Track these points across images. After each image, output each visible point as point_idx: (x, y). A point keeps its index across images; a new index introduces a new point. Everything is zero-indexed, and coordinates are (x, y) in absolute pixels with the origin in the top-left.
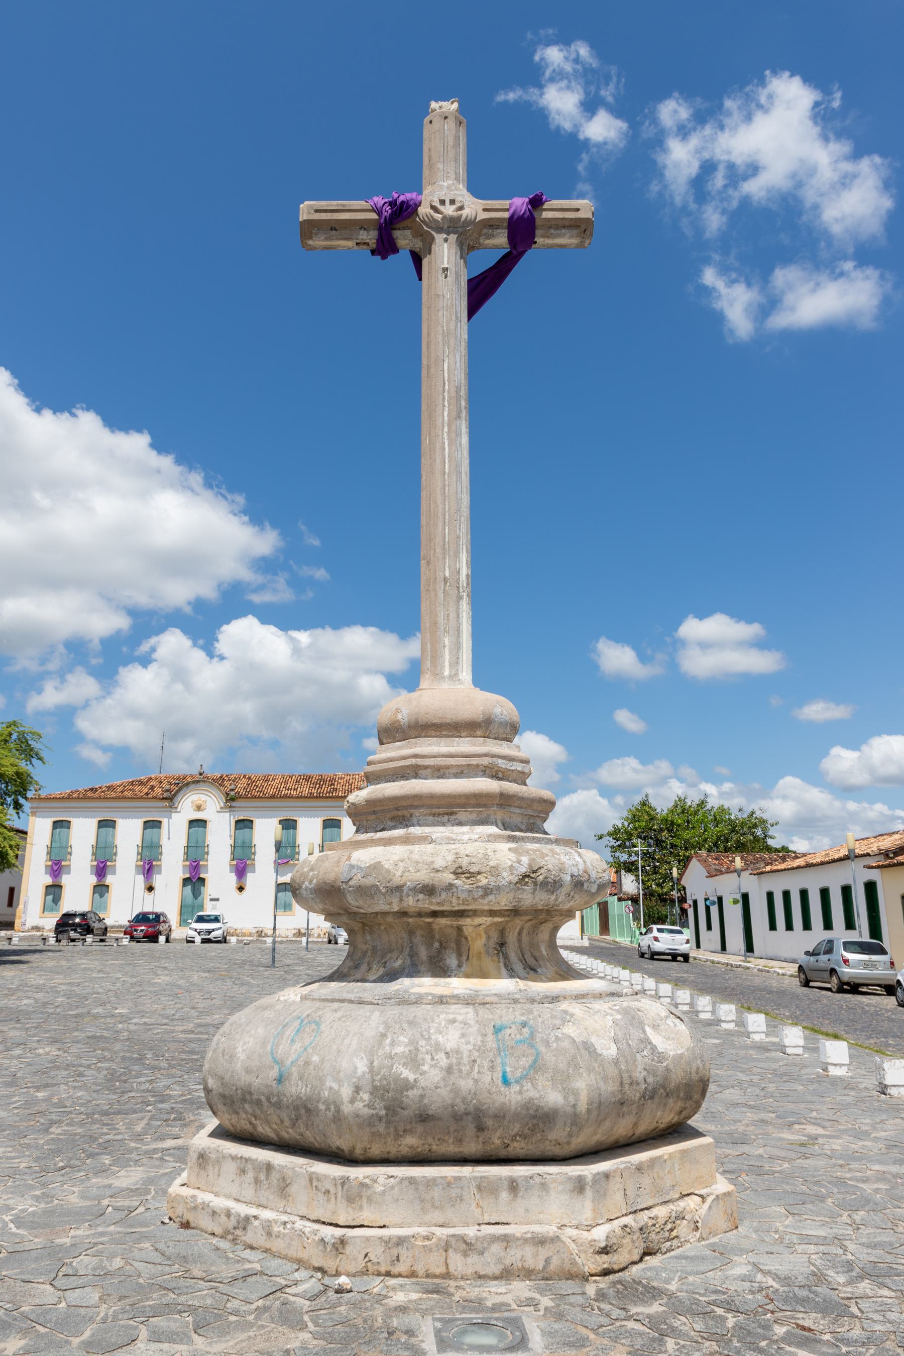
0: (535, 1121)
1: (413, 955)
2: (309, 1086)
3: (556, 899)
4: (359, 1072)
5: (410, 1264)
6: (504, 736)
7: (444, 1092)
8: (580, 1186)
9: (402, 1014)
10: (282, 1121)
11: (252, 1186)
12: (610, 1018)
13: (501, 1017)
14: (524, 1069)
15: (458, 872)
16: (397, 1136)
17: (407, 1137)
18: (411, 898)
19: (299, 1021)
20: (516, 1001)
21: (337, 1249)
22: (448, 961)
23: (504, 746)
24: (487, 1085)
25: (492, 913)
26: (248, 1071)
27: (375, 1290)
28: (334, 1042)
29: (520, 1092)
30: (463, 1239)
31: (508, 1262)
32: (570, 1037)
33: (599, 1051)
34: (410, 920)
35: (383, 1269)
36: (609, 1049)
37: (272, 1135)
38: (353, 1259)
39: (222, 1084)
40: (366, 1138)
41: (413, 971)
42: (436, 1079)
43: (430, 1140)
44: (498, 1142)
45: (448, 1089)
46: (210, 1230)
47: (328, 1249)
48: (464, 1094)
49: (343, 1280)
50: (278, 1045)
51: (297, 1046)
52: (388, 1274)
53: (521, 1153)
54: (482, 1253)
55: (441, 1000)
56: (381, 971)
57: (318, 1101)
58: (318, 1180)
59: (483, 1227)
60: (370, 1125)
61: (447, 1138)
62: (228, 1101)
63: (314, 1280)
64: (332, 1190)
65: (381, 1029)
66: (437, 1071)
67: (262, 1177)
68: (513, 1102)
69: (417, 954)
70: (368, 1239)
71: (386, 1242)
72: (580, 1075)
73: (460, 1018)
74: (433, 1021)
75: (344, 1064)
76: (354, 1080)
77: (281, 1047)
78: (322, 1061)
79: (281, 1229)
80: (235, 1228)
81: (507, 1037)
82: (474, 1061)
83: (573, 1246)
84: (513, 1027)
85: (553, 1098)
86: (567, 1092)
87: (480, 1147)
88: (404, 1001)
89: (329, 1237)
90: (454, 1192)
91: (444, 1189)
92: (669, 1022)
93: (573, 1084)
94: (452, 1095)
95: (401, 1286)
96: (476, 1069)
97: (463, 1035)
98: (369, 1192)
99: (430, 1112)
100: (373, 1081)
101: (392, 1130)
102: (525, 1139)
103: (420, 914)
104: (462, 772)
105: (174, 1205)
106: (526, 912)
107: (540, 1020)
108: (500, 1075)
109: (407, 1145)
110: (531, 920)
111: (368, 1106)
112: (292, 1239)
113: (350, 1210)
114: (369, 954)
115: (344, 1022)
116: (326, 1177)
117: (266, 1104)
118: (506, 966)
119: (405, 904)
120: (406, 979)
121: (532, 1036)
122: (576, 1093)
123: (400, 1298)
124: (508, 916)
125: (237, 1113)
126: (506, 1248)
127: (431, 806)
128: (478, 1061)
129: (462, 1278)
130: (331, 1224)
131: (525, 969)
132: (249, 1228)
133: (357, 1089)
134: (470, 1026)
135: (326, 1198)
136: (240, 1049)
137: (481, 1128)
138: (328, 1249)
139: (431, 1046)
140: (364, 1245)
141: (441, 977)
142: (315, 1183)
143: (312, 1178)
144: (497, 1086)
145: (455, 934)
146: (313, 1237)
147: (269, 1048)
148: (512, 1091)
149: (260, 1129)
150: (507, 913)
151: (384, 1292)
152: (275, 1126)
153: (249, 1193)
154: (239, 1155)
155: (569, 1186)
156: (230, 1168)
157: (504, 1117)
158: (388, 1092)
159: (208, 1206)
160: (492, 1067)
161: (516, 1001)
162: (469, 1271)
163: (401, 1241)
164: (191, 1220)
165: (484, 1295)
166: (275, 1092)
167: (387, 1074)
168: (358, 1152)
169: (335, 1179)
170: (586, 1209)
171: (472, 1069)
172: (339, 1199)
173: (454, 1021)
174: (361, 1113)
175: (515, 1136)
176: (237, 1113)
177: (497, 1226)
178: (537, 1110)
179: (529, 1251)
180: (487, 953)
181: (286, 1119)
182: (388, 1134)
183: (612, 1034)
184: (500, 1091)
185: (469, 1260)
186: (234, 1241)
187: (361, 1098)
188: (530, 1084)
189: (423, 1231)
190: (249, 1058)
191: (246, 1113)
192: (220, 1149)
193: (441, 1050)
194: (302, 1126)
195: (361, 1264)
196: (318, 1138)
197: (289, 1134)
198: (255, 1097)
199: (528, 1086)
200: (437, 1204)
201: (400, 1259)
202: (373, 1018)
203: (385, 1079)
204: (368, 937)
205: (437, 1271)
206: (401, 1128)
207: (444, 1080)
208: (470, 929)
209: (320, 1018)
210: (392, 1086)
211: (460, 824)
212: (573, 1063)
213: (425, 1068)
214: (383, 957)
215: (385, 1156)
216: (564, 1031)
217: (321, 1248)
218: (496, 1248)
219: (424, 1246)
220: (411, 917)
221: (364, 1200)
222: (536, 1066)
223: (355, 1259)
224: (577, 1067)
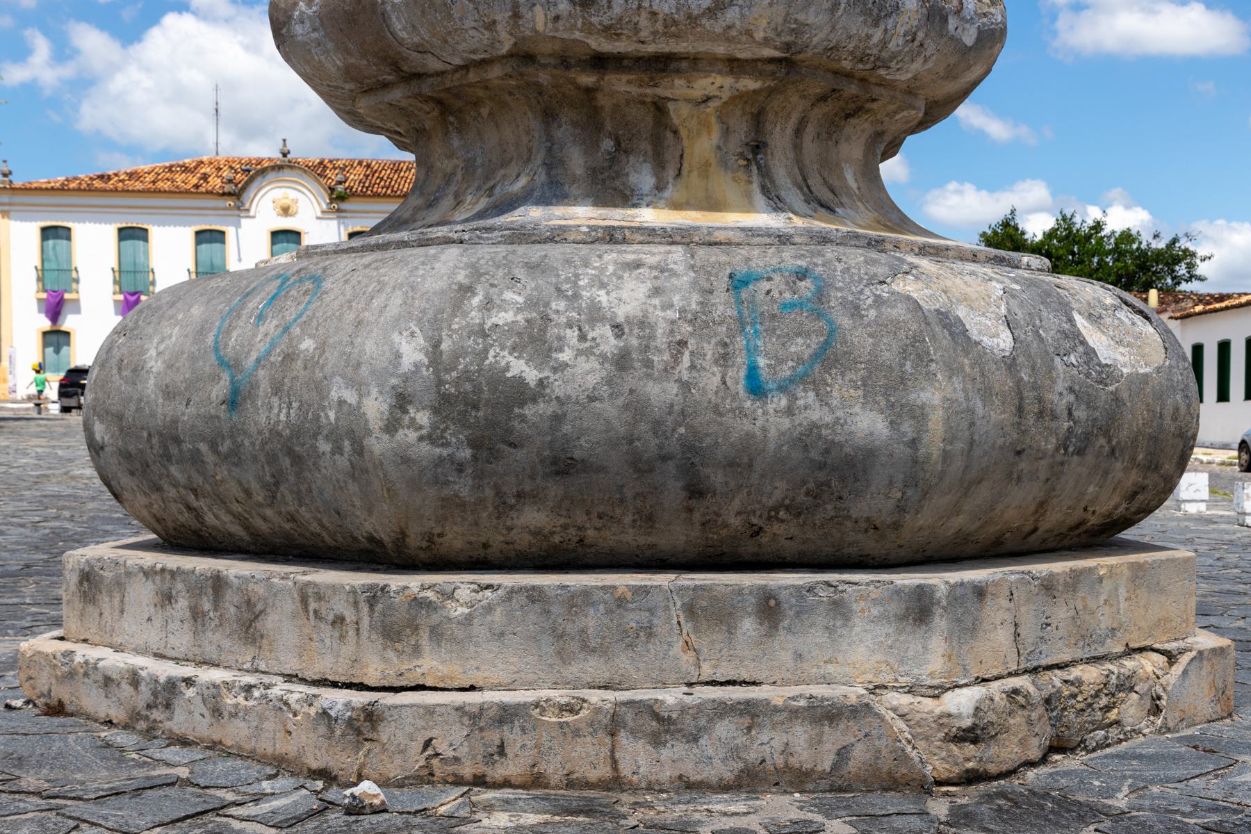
0: (821, 476)
2: (295, 405)
3: (884, 43)
4: (407, 363)
5: (531, 762)
7: (609, 409)
8: (919, 609)
9: (514, 252)
10: (248, 492)
11: (186, 626)
12: (1000, 286)
13: (749, 259)
14: (800, 361)
16: (503, 508)
17: (526, 508)
19: (279, 281)
21: (359, 732)
22: (633, 179)
24: (711, 395)
25: (734, 65)
26: (169, 393)
27: (442, 810)
28: (350, 308)
29: (790, 411)
30: (651, 710)
31: (753, 756)
32: (909, 298)
33: (975, 336)
35: (467, 771)
36: (997, 335)
37: (236, 529)
38: (399, 749)
39: (121, 430)
41: (554, 193)
42: (591, 381)
43: (580, 518)
44: (735, 522)
45: (620, 401)
46: (102, 715)
47: (338, 732)
49: (367, 787)
50: (228, 332)
51: (271, 326)
52: (480, 781)
53: (790, 549)
54: (694, 739)
55: (611, 236)
56: (483, 203)
57: (315, 436)
58: (320, 598)
59: (698, 688)
60: (436, 481)
61: (618, 512)
62: (138, 466)
63: (304, 792)
64: (350, 616)
65: (462, 277)
66: (593, 363)
67: (207, 605)
68: (773, 433)
69: (562, 162)
70: (430, 710)
71: (474, 718)
72: (930, 377)
74: (586, 265)
75: (370, 347)
76: (394, 381)
77: (235, 334)
78: (322, 347)
79: (241, 699)
80: (149, 707)
81: (761, 296)
82: (682, 343)
83: (900, 724)
84: (777, 278)
85: (868, 424)
86: (898, 412)
87: (695, 533)
88: (522, 236)
89: (340, 706)
90: (632, 619)
91: (609, 612)
93: (912, 396)
94: (627, 416)
95: (507, 802)
96: (686, 360)
97: (656, 291)
98: (435, 618)
99: (577, 454)
100: (440, 383)
101: (489, 493)
102: (799, 515)
103: (564, 61)
105: (32, 672)
107: (840, 267)
108: (743, 373)
109: (526, 528)
111: (430, 438)
112: (262, 718)
113: (391, 654)
114: (459, 176)
115: (377, 269)
116: (334, 588)
117: (210, 458)
118: (765, 191)
120: (534, 208)
121: (820, 295)
122: (919, 414)
125: (159, 489)
126: (749, 729)
128: (692, 343)
129: (649, 788)
130: (349, 686)
131: (807, 202)
132: (178, 704)
133: (402, 401)
134: (674, 274)
135: (337, 634)
136: (153, 352)
137: (696, 491)
138: (338, 732)
140: (421, 723)
141: (615, 206)
142: (313, 605)
143: (305, 595)
145: (649, 120)
146: (306, 709)
147: (210, 340)
148: (771, 408)
149: (210, 519)
150: (770, 67)
151: (463, 813)
152: (237, 508)
153: (182, 640)
154: (159, 566)
155: (895, 608)
156: (142, 593)
157: (750, 465)
158: (476, 407)
159: (95, 668)
160: (725, 357)
162: (666, 774)
163: (506, 715)
164: (66, 699)
165: (697, 816)
166: (225, 428)
167: (474, 368)
168: (414, 541)
169: (353, 591)
170: (932, 654)
171: (676, 358)
172: (365, 633)
173: (637, 265)
174: (412, 453)
175: (776, 509)
176: (159, 489)
177: (730, 688)
178: (827, 451)
179: (800, 735)
180: (724, 163)
181: (254, 486)
183: (1003, 310)
184: (741, 409)
185: (665, 753)
186: (150, 733)
187: (413, 420)
188: (811, 394)
189: (560, 696)
190: (170, 366)
191: (176, 485)
192: (121, 561)
193: (602, 319)
194: (289, 498)
195: (416, 762)
196: (325, 521)
197: (269, 521)
198: (187, 446)
200: (593, 644)
201: (507, 750)
202: (443, 257)
203: (468, 379)
204: (456, 142)
205: (593, 775)
206: (510, 489)
207: (609, 382)
209: (325, 269)
210: (486, 395)
212: (915, 350)
213: (565, 356)
214: (487, 178)
215: (482, 553)
216: (894, 286)
217: (323, 730)
218: (725, 729)
220: (545, 66)
221: (425, 636)
222: (830, 356)
223: (402, 752)
224: (923, 359)
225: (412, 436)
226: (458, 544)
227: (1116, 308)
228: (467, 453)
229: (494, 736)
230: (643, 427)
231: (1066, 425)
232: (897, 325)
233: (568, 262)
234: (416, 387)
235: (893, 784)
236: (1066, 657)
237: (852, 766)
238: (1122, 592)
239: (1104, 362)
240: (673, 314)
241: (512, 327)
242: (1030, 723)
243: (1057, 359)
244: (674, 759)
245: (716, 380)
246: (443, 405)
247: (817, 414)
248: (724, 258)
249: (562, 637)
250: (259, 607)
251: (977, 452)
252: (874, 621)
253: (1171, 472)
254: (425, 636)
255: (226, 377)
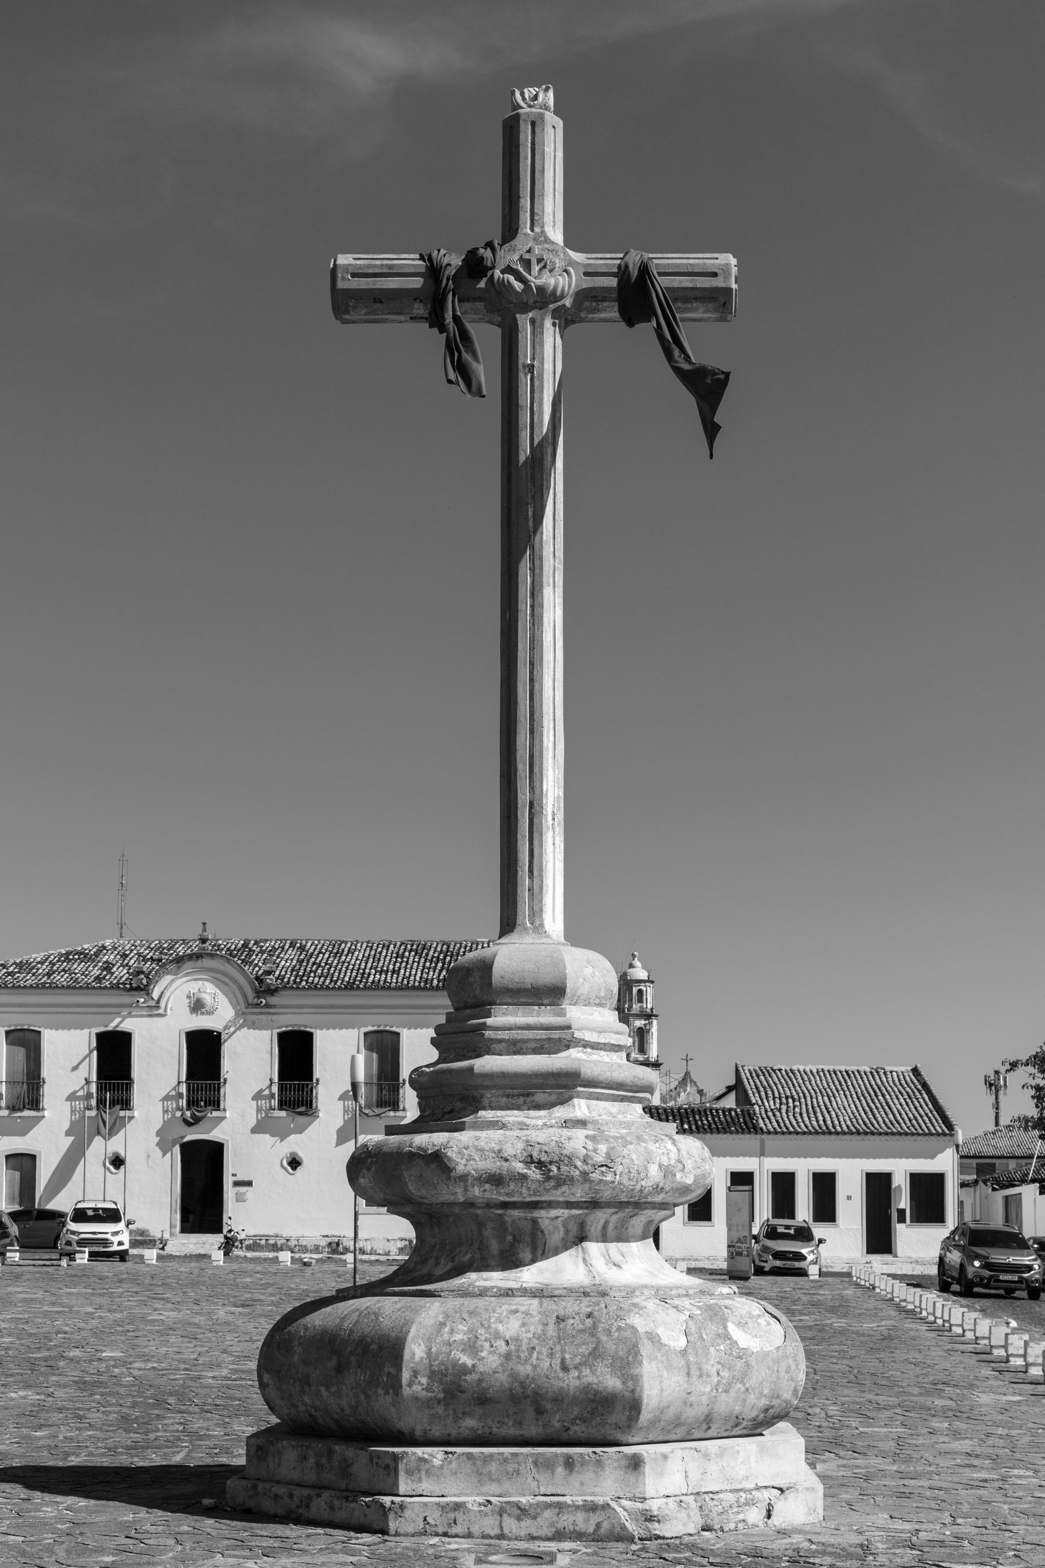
0: (594, 1405)
1: (483, 1248)
4: (417, 1358)
6: (598, 1001)
7: (503, 1377)
10: (343, 1410)
14: (583, 1356)
15: (529, 1161)
16: (457, 1419)
18: (476, 1188)
20: (586, 1294)
22: (521, 1255)
23: (596, 1014)
25: (569, 1205)
29: (579, 1378)
30: (518, 1506)
31: (560, 1526)
34: (479, 1212)
35: (440, 1530)
36: (678, 1340)
40: (425, 1420)
41: (483, 1266)
42: (495, 1365)
43: (490, 1423)
44: (557, 1425)
48: (522, 1379)
52: (445, 1535)
54: (535, 1518)
55: (509, 1293)
65: (440, 1318)
67: (324, 1461)
69: (487, 1247)
70: (425, 1504)
71: (443, 1508)
73: (522, 1309)
80: (298, 1507)
82: (533, 1348)
87: (540, 1430)
90: (511, 1467)
92: (762, 1321)
94: (509, 1380)
96: (535, 1355)
97: (524, 1325)
98: (428, 1466)
99: (488, 1396)
100: (431, 1366)
101: (451, 1412)
103: (489, 1205)
104: (542, 1047)
106: (608, 1205)
108: (559, 1361)
109: (466, 1427)
110: (616, 1213)
113: (409, 1481)
118: (584, 1260)
119: (470, 1195)
121: (595, 1326)
123: (454, 1546)
124: (587, 1208)
127: (504, 1087)
128: (537, 1348)
129: (516, 1539)
137: (540, 1412)
139: (490, 1334)
142: (375, 1460)
144: (555, 1371)
145: (530, 1227)
148: (571, 1376)
149: (321, 1421)
150: (586, 1205)
155: (624, 1463)
158: (446, 1376)
160: (551, 1354)
161: (586, 1294)
163: (458, 1507)
168: (418, 1433)
171: (531, 1355)
175: (575, 1419)
178: (595, 1395)
179: (580, 1517)
182: (447, 1416)
185: (523, 1524)
191: (305, 1405)
199: (586, 1371)
202: (433, 1308)
204: (436, 1231)
205: (493, 1533)
207: (502, 1365)
208: (547, 1222)
211: (538, 1107)
213: (484, 1354)
218: (548, 1514)
219: (479, 1511)
220: (479, 1208)
221: (423, 1473)
225: (420, 1388)
226: (437, 1434)
227: (759, 1316)
228: (441, 1395)
229: (451, 1516)
230: (516, 1384)
231: (716, 1380)
232: (627, 1339)
233: (487, 1310)
234: (420, 1368)
235: (619, 1539)
236: (717, 1489)
237: (602, 1531)
238: (753, 1459)
239: (741, 1346)
240: (530, 1335)
241: (462, 1342)
242: (689, 1516)
243: (712, 1349)
244: (527, 1526)
245: (547, 1364)
246: (433, 1375)
247: (591, 1379)
248: (554, 1307)
249: (481, 1477)
250: (350, 1461)
251: (665, 1394)
252: (615, 1468)
253: (789, 1398)
254: (423, 1473)
255: (335, 1358)
